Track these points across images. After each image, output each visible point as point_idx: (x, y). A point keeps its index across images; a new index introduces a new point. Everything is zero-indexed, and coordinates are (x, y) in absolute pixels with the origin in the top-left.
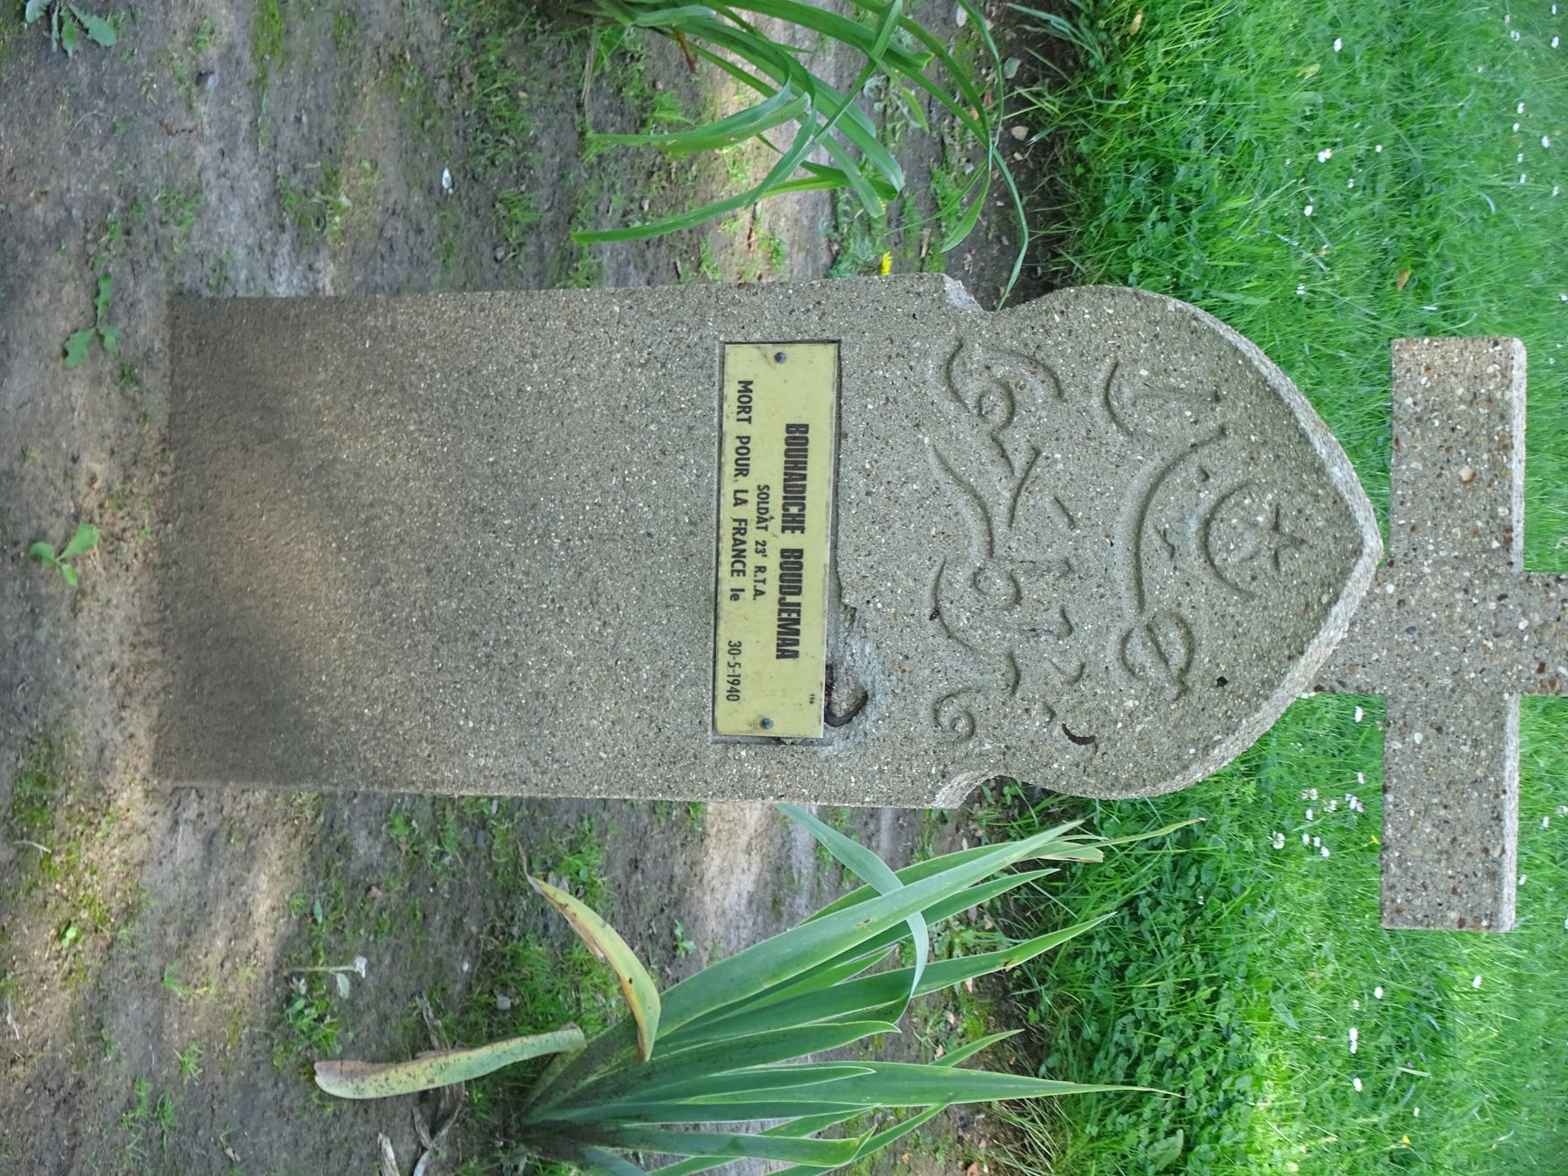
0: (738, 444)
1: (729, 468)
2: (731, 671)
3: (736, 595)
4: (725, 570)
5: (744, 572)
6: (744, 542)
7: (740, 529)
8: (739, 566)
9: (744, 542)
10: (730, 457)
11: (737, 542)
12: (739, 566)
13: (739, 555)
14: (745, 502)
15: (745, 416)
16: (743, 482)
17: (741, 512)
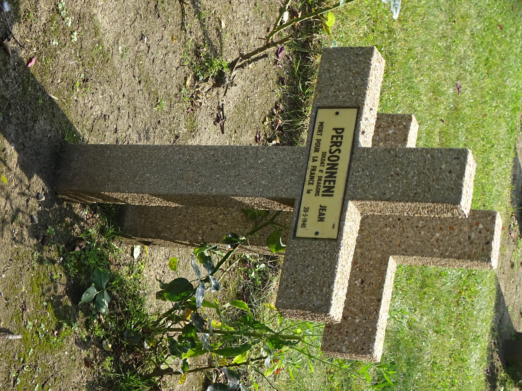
0: (316, 142)
2: (303, 217)
3: (309, 192)
4: (307, 183)
5: (313, 184)
6: (314, 174)
7: (314, 169)
8: (311, 182)
9: (314, 174)
10: (313, 146)
11: (311, 174)
12: (311, 182)
13: (312, 178)
14: (316, 160)
15: (319, 133)
16: (316, 154)
17: (315, 164)
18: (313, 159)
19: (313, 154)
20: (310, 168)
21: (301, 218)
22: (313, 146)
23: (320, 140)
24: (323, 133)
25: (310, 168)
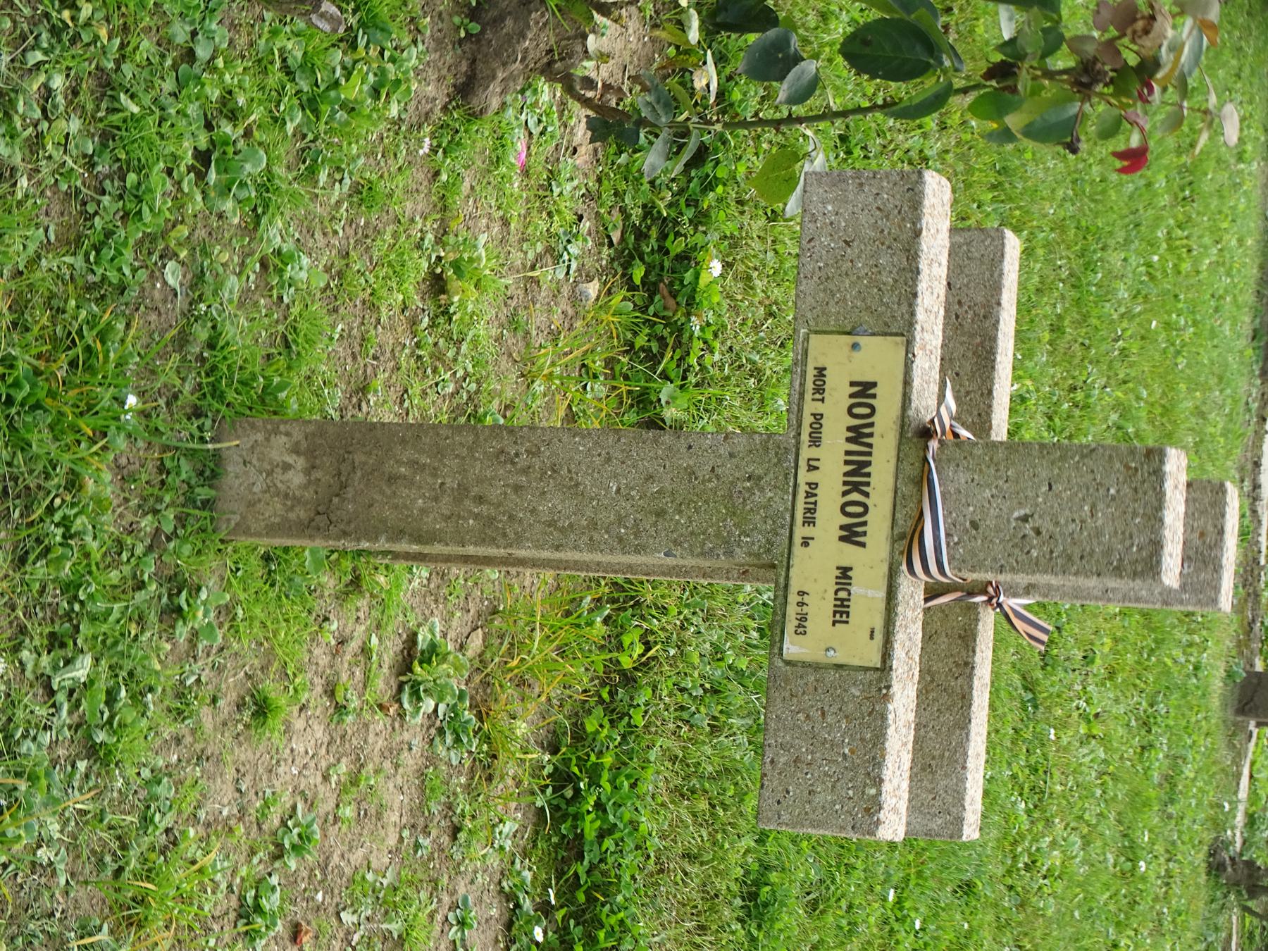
0: (812, 419)
1: (805, 437)
3: (805, 544)
10: (806, 430)
13: (811, 510)
14: (816, 468)
15: (818, 396)
16: (814, 452)
17: (813, 477)
18: (809, 466)
19: (806, 452)
20: (803, 488)
21: (792, 610)
22: (806, 430)
23: (822, 415)
24: (826, 395)
25: (803, 488)
